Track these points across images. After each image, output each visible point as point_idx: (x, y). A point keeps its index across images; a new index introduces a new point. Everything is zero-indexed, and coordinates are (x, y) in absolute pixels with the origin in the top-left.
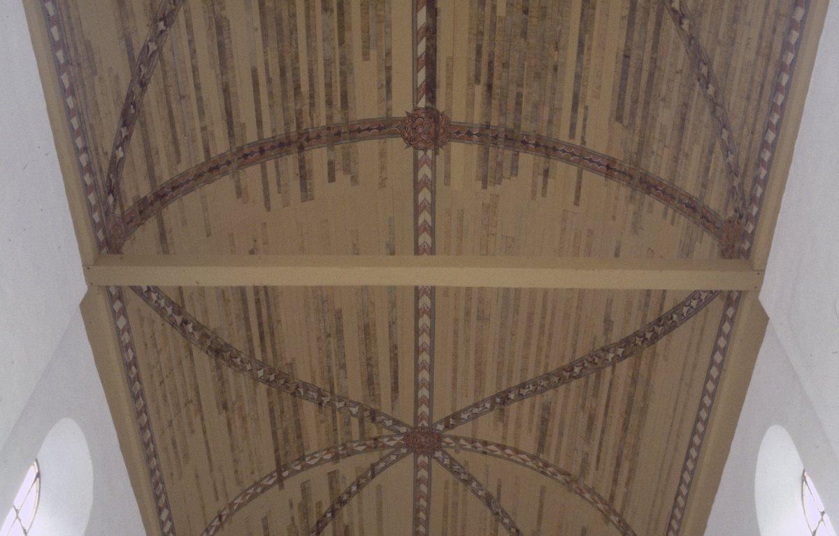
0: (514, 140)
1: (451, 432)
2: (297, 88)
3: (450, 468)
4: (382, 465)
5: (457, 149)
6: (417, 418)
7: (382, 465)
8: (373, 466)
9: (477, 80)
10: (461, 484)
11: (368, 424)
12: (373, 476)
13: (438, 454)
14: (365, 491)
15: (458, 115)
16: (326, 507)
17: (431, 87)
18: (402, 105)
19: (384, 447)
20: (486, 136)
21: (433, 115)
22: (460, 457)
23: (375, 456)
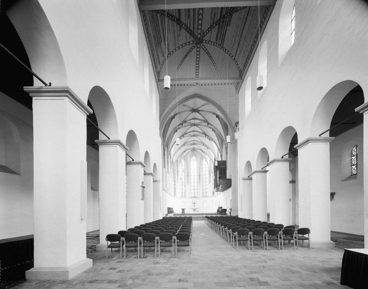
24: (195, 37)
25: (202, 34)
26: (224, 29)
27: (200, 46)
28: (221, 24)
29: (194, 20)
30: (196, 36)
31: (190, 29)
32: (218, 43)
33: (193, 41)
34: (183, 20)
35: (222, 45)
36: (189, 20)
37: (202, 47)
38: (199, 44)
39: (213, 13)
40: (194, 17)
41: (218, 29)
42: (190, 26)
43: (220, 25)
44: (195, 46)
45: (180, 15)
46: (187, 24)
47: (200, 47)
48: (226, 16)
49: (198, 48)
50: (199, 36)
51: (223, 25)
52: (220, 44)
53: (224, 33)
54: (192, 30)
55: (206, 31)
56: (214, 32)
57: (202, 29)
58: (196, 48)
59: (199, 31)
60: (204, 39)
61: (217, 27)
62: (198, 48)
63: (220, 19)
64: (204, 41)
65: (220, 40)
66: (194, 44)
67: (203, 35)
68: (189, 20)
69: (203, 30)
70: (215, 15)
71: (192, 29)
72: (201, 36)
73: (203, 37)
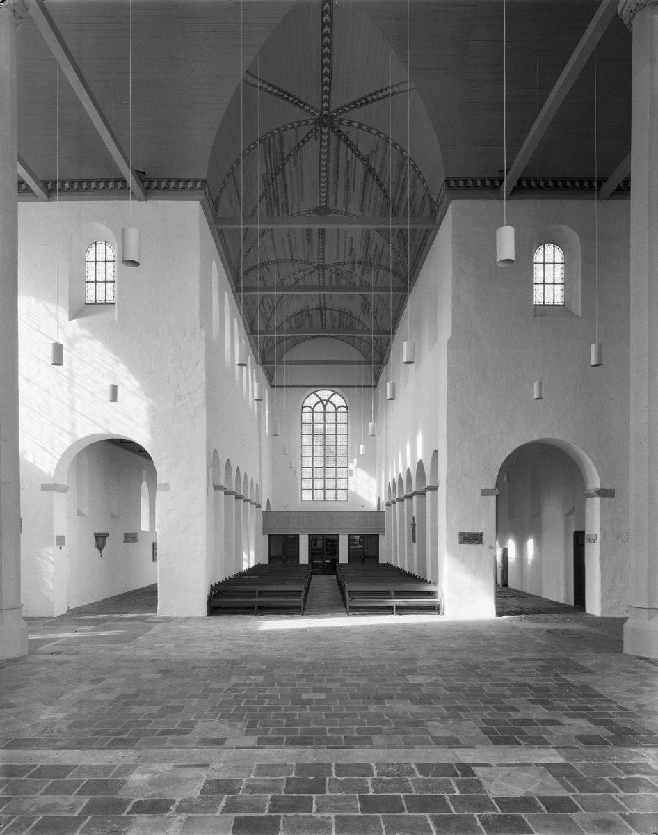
15: (315, 312)
16: (357, 266)
17: (321, 312)
18: (328, 312)
24: (335, 130)
25: (319, 133)
27: (321, 112)
28: (279, 162)
30: (333, 131)
31: (347, 145)
32: (277, 137)
33: (341, 124)
34: (360, 169)
35: (267, 141)
36: (349, 158)
37: (316, 110)
38: (325, 116)
39: (299, 165)
40: (338, 158)
41: (282, 153)
45: (366, 174)
46: (354, 156)
47: (323, 109)
48: (274, 177)
49: (328, 109)
50: (325, 130)
53: (269, 160)
56: (290, 143)
57: (319, 141)
58: (333, 108)
59: (325, 138)
61: (286, 152)
62: (328, 109)
63: (283, 165)
64: (312, 122)
65: (275, 143)
70: (295, 163)
71: (343, 145)
73: (316, 129)
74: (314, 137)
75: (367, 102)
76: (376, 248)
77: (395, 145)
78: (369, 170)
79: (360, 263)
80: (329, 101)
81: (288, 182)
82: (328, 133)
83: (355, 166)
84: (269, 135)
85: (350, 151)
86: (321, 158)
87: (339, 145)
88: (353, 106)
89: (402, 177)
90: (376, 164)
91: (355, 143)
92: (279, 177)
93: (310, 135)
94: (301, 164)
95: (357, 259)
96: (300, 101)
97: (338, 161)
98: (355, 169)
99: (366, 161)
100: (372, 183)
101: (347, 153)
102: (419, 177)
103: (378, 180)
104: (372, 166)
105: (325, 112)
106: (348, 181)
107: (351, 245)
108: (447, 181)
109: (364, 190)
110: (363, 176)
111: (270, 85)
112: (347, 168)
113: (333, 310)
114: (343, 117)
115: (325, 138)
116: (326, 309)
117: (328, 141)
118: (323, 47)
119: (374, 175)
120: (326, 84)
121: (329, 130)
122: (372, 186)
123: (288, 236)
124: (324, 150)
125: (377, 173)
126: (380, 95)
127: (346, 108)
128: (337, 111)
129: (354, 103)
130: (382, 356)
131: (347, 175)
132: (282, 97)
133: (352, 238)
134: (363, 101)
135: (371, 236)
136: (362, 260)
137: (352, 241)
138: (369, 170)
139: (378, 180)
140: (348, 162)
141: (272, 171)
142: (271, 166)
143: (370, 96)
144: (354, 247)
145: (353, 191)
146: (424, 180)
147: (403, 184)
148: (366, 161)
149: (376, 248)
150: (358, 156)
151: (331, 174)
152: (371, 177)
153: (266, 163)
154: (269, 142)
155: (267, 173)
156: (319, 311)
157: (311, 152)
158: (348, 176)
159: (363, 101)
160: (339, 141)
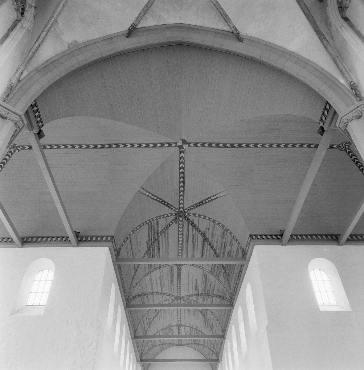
0: (167, 328)
1: (173, 300)
2: (196, 332)
3: (173, 296)
4: (187, 296)
5: (175, 324)
6: (180, 301)
7: (187, 296)
8: (189, 296)
9: (173, 329)
10: (170, 293)
11: (190, 302)
12: (189, 295)
13: (175, 297)
14: (191, 294)
16: (200, 296)
17: (179, 328)
18: (183, 328)
19: (187, 298)
20: (171, 326)
21: (178, 326)
22: (171, 297)
23: (188, 298)
24: (187, 218)
25: (178, 221)
26: (151, 235)
28: (156, 235)
29: (188, 232)
30: (185, 219)
31: (193, 226)
32: (155, 221)
34: (200, 238)
35: (150, 223)
36: (194, 233)
37: (176, 209)
38: (181, 211)
39: (167, 237)
40: (188, 234)
42: (193, 230)
43: (157, 234)
44: (186, 210)
46: (197, 232)
47: (180, 208)
48: (153, 243)
49: (183, 208)
50: (181, 219)
51: (153, 235)
52: (152, 222)
54: (190, 225)
55: (172, 223)
58: (185, 208)
59: (181, 223)
60: (175, 217)
63: (158, 237)
66: (189, 212)
67: (175, 220)
68: (194, 233)
69: (176, 224)
70: (165, 237)
71: (191, 227)
72: (179, 219)
74: (175, 223)
75: (203, 204)
76: (211, 284)
77: (219, 224)
78: (205, 239)
79: (201, 294)
80: (183, 204)
81: (161, 246)
82: (183, 220)
83: (198, 237)
84: (151, 220)
85: (194, 229)
86: (179, 233)
87: (189, 226)
88: (195, 206)
89: (224, 240)
90: (209, 236)
91: (197, 225)
92: (156, 244)
93: (173, 221)
94: (168, 237)
95: (200, 292)
96: (168, 204)
97: (188, 235)
98: (197, 239)
99: (203, 234)
100: (207, 246)
101: (193, 231)
102: (234, 238)
103: (210, 244)
104: (207, 237)
105: (181, 210)
106: (194, 246)
107: (196, 284)
108: (251, 236)
109: (203, 251)
110: (202, 243)
111: (152, 195)
112: (193, 239)
113: (186, 326)
114: (190, 212)
115: (181, 223)
116: (182, 326)
117: (183, 224)
118: (180, 178)
119: (208, 242)
120: (182, 182)
121: (183, 219)
122: (207, 247)
123: (160, 278)
124: (180, 230)
125: (210, 240)
126: (210, 199)
127: (192, 207)
128: (188, 209)
129: (196, 204)
130: (218, 355)
131: (193, 242)
132: (159, 201)
133: (196, 279)
134: (201, 203)
135: (208, 277)
136: (203, 293)
137: (196, 281)
138: (205, 239)
139: (210, 244)
140: (193, 236)
141: (152, 240)
142: (151, 236)
143: (205, 200)
144: (197, 285)
145: (197, 252)
146: (237, 240)
147: (225, 245)
148: (203, 234)
149: (211, 284)
150: (199, 232)
151: (184, 243)
152: (206, 243)
153: (149, 235)
154: (151, 224)
155: (149, 240)
156: (177, 327)
157: (174, 229)
158: (194, 243)
159: (201, 203)
160: (189, 224)
